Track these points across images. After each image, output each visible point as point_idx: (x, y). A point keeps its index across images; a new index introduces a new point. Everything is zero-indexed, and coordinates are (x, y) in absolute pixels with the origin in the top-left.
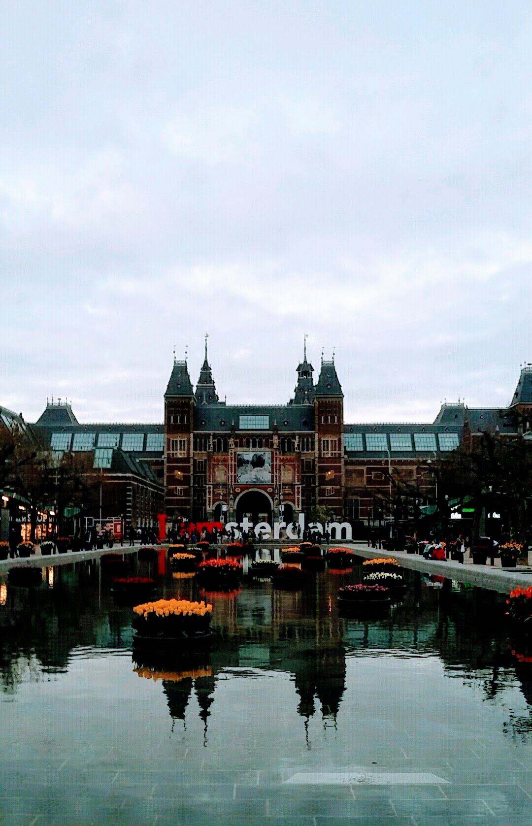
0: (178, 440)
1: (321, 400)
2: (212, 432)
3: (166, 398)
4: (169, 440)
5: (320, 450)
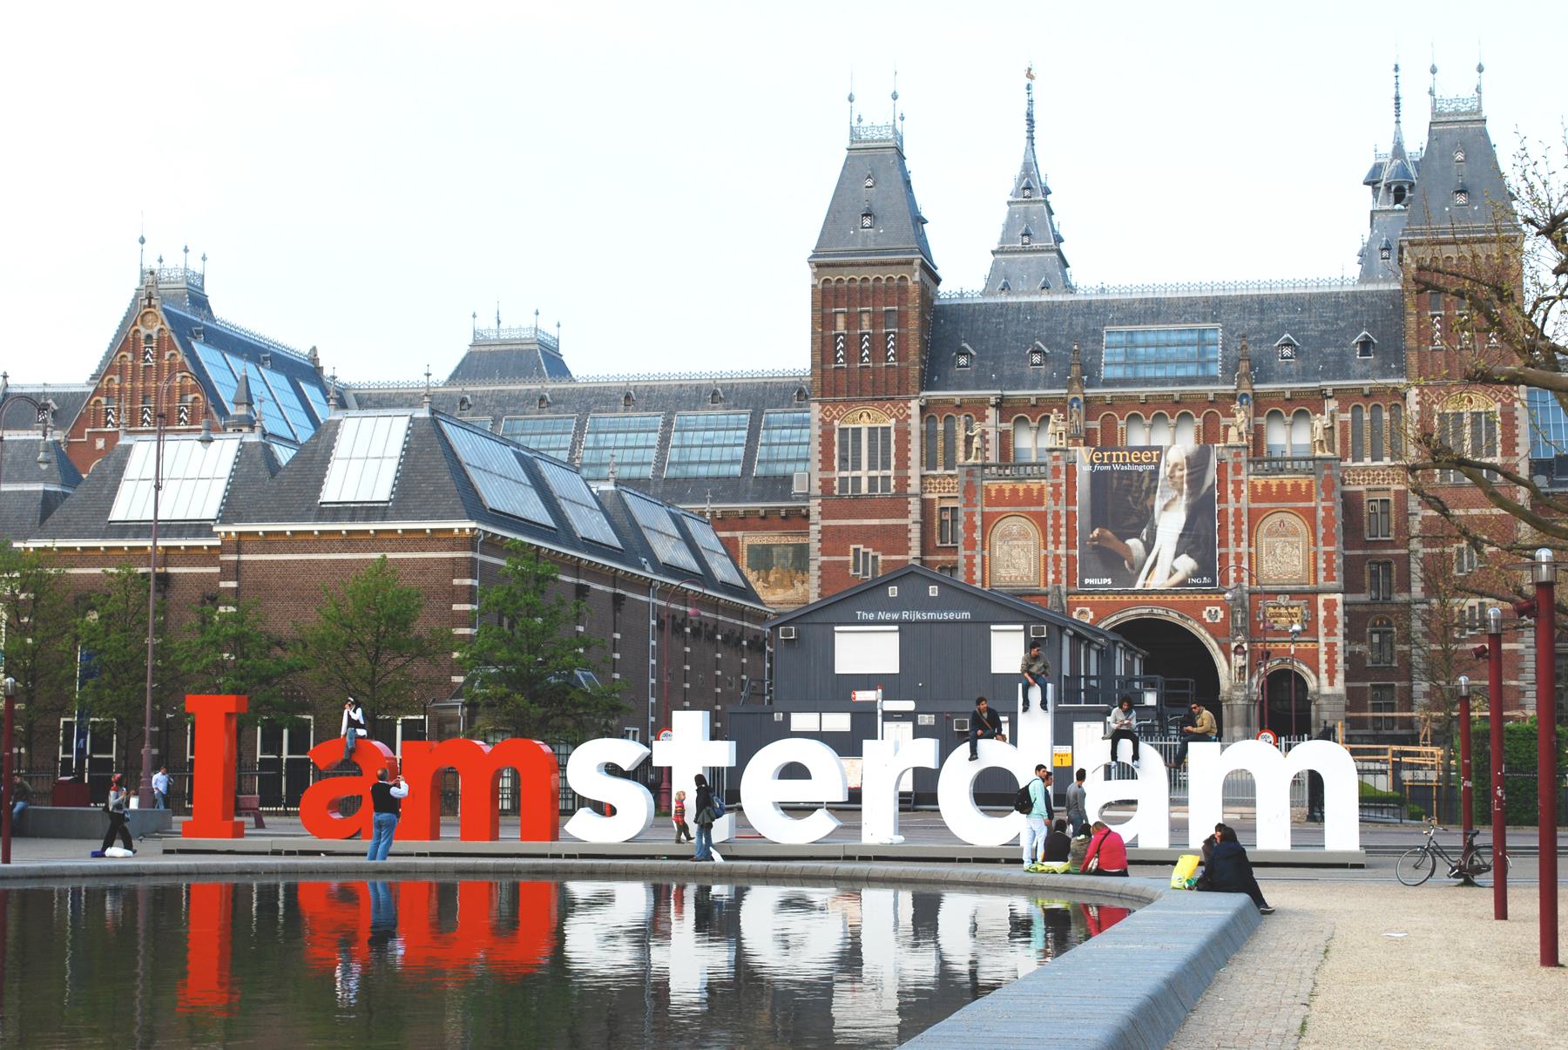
0: (865, 425)
2: (992, 394)
3: (820, 265)
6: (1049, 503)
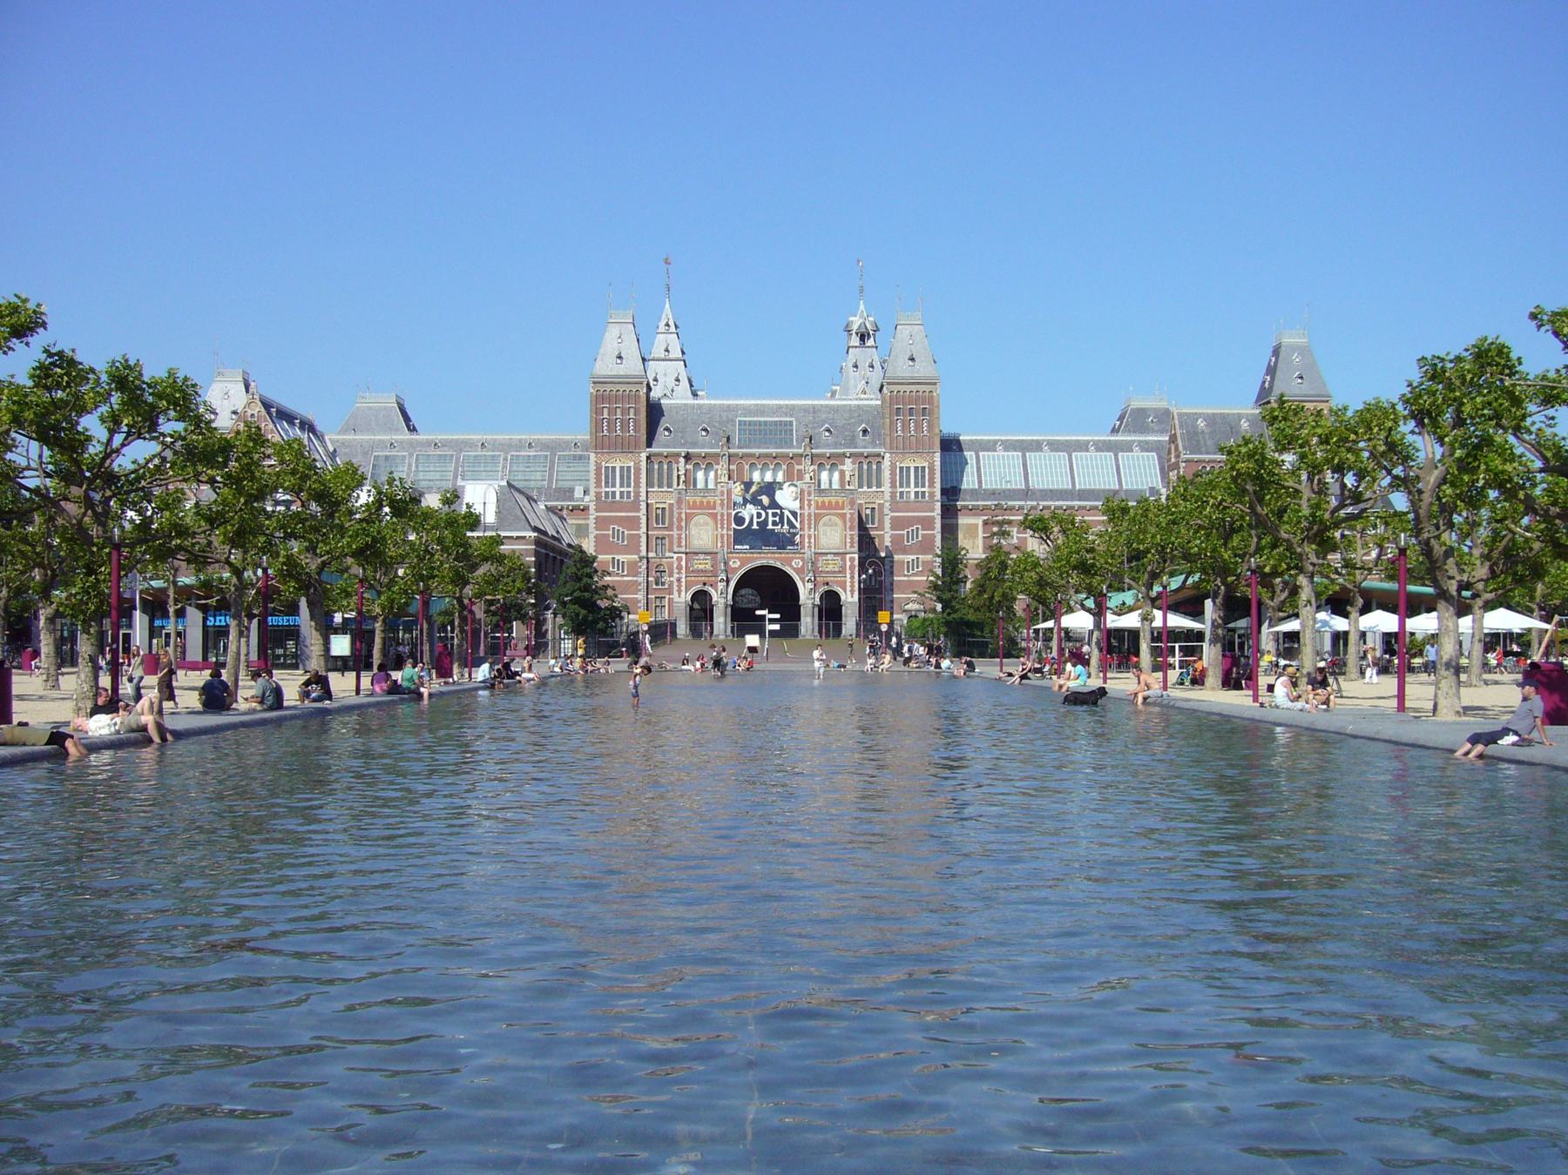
0: (618, 465)
1: (895, 388)
4: (598, 470)
5: (893, 485)
6: (719, 509)
